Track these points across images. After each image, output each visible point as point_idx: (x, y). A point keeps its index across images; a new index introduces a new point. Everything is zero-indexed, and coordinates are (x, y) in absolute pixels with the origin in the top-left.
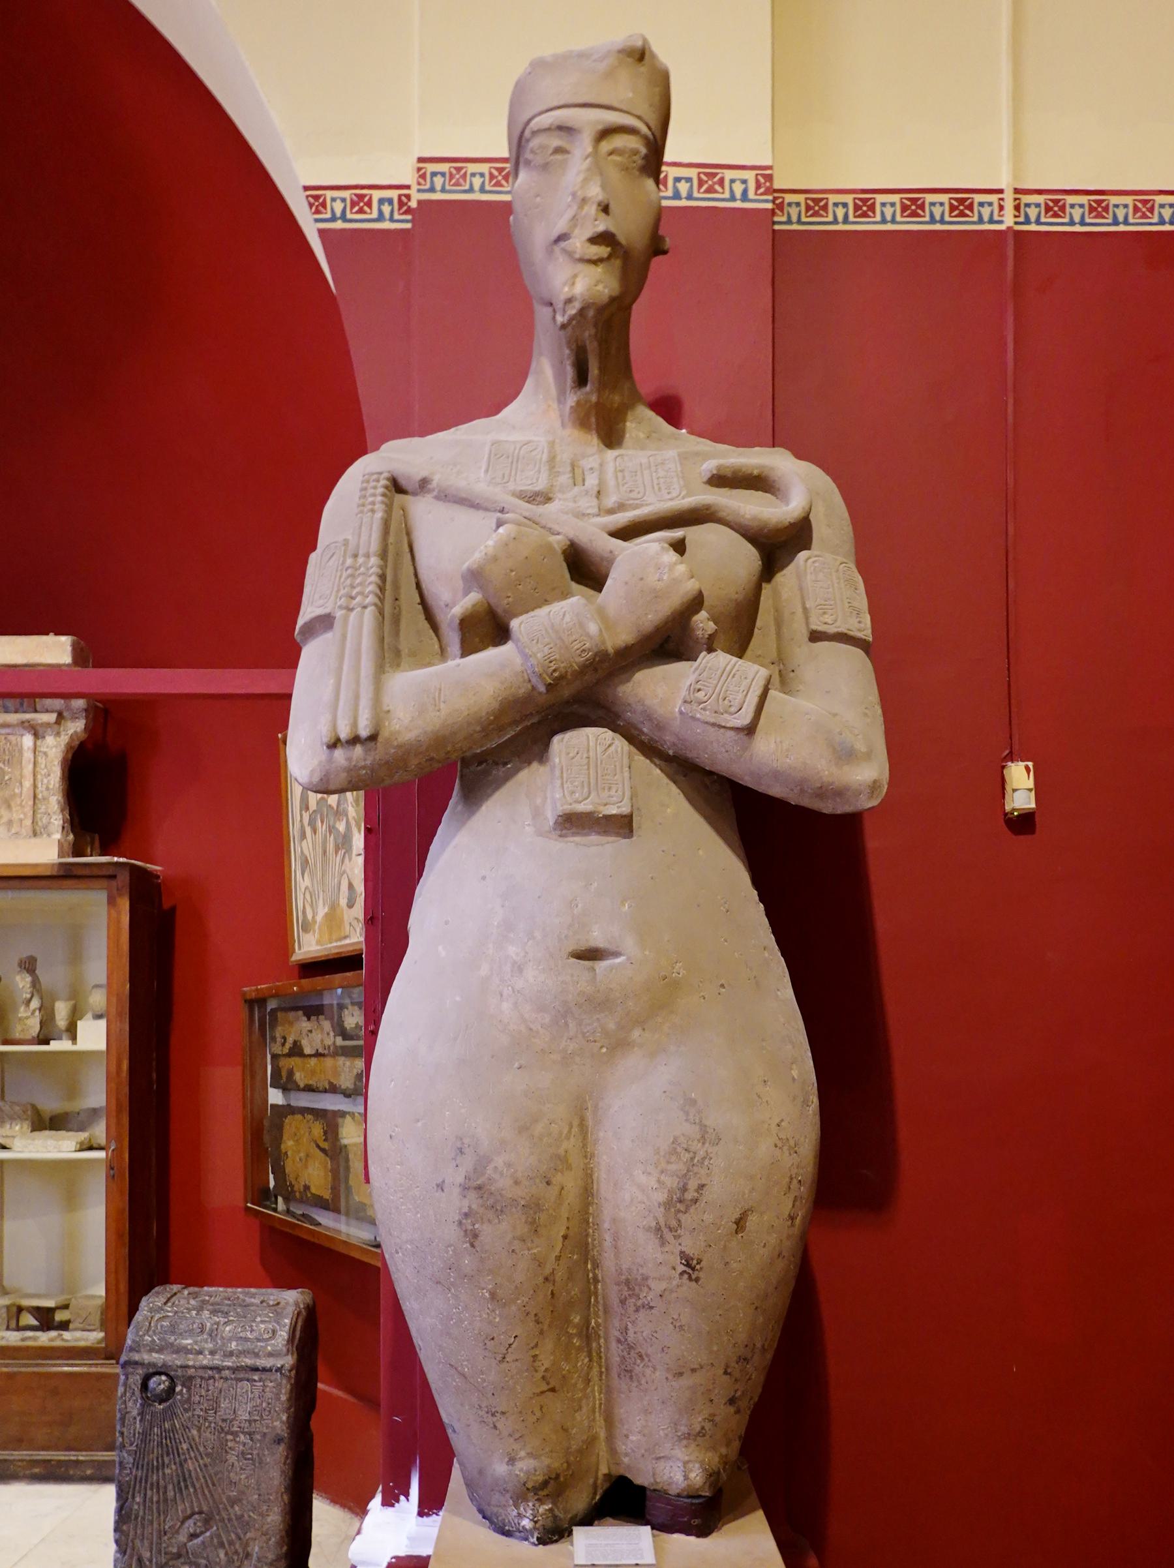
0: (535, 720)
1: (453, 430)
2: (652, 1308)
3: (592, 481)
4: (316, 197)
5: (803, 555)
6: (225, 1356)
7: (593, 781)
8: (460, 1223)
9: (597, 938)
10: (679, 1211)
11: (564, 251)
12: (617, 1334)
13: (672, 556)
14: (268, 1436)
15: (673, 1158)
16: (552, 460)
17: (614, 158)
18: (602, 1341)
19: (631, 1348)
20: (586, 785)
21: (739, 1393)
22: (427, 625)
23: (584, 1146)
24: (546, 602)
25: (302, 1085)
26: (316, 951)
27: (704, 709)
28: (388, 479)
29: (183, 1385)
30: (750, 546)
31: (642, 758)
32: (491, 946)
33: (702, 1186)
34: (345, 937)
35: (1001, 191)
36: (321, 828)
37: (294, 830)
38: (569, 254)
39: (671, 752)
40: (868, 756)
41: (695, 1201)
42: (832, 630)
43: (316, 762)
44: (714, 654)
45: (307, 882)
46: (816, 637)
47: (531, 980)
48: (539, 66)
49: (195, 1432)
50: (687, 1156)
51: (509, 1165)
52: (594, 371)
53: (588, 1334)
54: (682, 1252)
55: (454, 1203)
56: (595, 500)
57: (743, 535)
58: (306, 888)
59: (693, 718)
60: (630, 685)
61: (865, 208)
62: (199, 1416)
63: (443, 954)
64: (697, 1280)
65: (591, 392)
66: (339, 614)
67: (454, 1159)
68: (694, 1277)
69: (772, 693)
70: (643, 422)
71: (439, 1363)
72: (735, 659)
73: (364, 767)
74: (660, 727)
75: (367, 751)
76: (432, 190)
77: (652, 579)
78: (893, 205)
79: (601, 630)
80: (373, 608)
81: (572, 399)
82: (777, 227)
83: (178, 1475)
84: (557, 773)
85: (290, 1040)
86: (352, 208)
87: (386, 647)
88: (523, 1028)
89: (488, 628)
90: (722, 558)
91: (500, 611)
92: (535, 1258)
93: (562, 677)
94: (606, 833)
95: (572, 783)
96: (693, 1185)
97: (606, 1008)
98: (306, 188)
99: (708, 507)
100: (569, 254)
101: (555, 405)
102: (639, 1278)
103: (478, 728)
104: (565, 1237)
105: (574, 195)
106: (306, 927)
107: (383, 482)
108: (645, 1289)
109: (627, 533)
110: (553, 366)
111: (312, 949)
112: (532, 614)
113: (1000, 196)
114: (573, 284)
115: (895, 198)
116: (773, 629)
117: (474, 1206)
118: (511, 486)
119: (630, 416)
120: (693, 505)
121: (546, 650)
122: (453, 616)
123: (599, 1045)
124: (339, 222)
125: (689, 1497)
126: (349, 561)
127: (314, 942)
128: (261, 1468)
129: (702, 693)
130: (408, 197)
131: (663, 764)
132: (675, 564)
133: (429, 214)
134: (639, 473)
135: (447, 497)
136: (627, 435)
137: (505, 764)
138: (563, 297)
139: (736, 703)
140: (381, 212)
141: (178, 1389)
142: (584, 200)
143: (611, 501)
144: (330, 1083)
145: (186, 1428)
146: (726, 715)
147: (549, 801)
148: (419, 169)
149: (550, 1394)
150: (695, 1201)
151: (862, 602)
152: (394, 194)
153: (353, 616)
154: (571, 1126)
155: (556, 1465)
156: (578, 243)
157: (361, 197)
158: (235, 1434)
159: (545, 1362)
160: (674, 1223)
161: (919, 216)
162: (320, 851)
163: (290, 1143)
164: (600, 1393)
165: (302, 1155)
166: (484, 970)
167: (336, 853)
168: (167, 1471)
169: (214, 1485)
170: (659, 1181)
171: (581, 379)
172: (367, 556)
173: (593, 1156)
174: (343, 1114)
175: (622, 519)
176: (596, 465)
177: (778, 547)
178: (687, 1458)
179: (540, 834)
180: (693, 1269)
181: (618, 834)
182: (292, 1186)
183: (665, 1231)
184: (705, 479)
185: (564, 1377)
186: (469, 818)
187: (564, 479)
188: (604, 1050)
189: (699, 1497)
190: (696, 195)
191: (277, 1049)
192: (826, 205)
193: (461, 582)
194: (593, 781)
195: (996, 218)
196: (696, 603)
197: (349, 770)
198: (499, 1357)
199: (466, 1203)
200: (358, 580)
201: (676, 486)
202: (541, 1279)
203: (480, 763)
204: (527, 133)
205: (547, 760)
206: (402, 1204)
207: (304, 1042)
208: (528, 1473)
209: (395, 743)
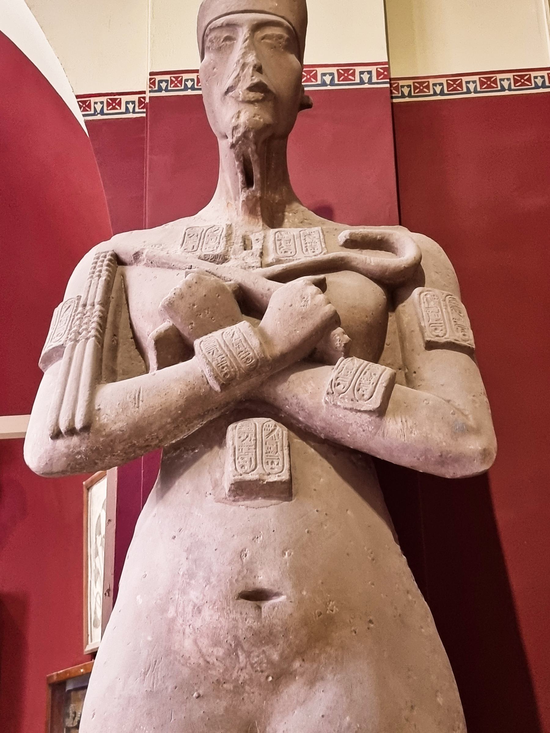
3: (257, 247)
4: (84, 101)
5: (417, 291)
7: (259, 457)
16: (229, 236)
20: (253, 460)
24: (221, 327)
28: (112, 255)
30: (376, 285)
31: (300, 441)
39: (322, 436)
40: (477, 431)
42: (443, 340)
46: (430, 346)
47: (208, 619)
52: (257, 175)
56: (259, 258)
57: (371, 278)
60: (286, 384)
61: (455, 86)
65: (256, 189)
70: (296, 213)
73: (79, 453)
76: (160, 90)
78: (474, 82)
79: (261, 344)
80: (94, 338)
81: (243, 196)
82: (395, 101)
86: (108, 106)
87: (103, 367)
88: (201, 661)
90: (354, 292)
93: (232, 379)
95: (242, 459)
98: (77, 97)
99: (342, 259)
103: (169, 420)
107: (108, 257)
112: (210, 335)
115: (476, 78)
116: (398, 344)
118: (198, 253)
123: (266, 674)
124: (99, 115)
129: (341, 386)
130: (144, 98)
131: (317, 445)
133: (156, 107)
134: (292, 241)
135: (152, 263)
137: (193, 450)
140: (127, 108)
143: (270, 259)
148: (150, 79)
151: (466, 322)
152: (135, 98)
156: (241, 90)
157: (114, 100)
166: (171, 613)
171: (248, 182)
175: (277, 268)
176: (261, 238)
177: (398, 285)
181: (279, 498)
184: (342, 243)
188: (270, 679)
192: (428, 85)
193: (158, 317)
194: (259, 457)
196: (334, 320)
209: (104, 433)
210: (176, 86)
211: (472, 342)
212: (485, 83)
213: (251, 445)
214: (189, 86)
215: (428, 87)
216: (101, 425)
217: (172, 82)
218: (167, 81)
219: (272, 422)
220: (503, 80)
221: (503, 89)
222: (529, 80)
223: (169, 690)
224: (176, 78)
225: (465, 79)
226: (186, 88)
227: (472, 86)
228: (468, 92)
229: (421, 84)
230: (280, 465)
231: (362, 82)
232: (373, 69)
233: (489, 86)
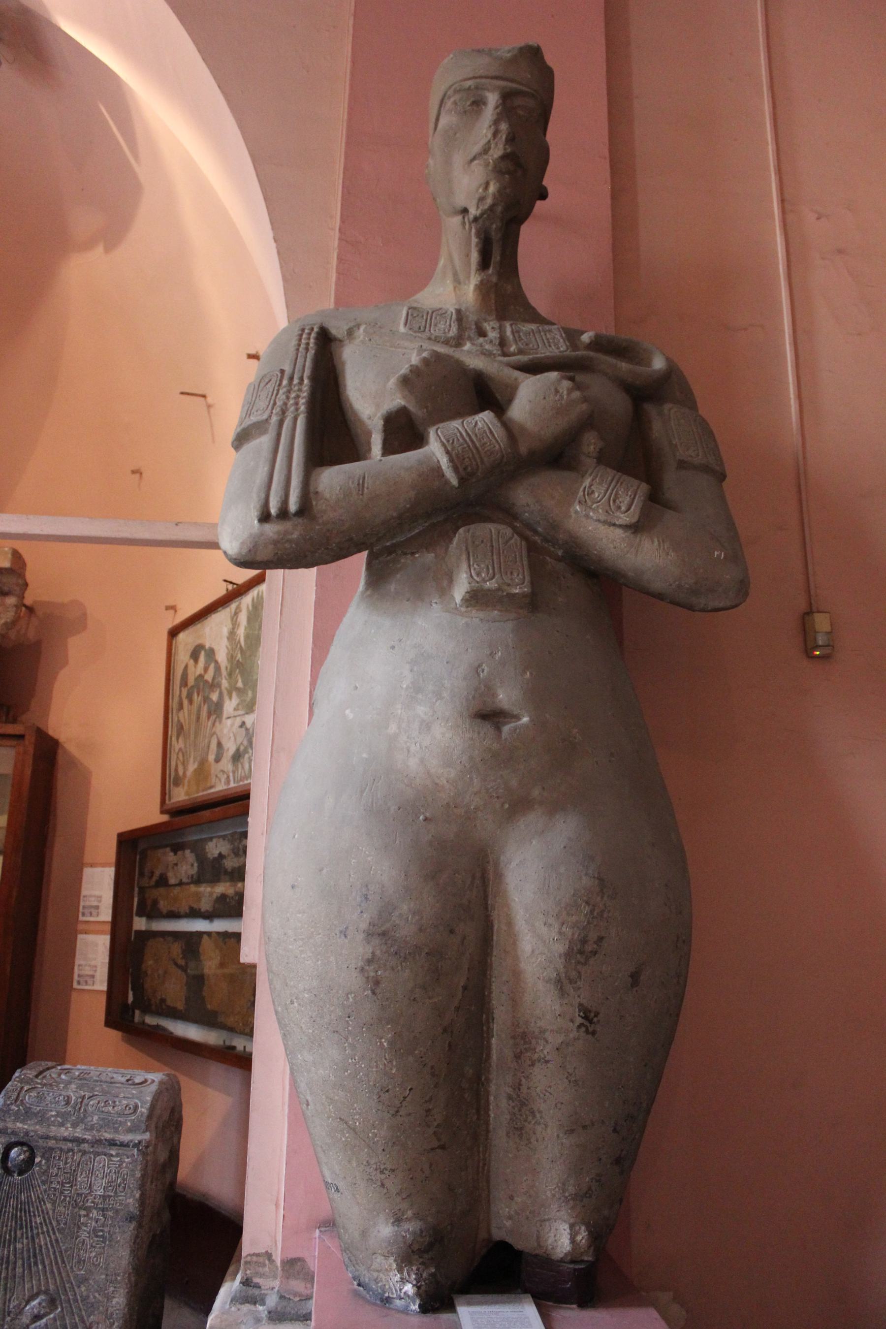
2: (547, 1062)
6: (86, 1129)
8: (362, 970)
10: (579, 962)
12: (509, 1090)
14: (121, 1213)
21: (624, 1152)
25: (165, 911)
26: (184, 801)
29: (43, 1157)
32: (399, 706)
33: (601, 939)
34: (211, 787)
41: (595, 953)
45: (181, 744)
49: (49, 1206)
54: (580, 1005)
58: (180, 750)
62: (55, 1189)
63: (351, 716)
64: (594, 1033)
68: (591, 1030)
71: (328, 1118)
83: (29, 1251)
85: (157, 873)
96: (593, 936)
102: (537, 1031)
104: (465, 988)
108: (542, 1042)
111: (180, 799)
117: (378, 952)
125: (572, 1262)
127: (183, 794)
128: (110, 1246)
141: (37, 1160)
144: (191, 908)
145: (41, 1201)
149: (439, 1151)
150: (595, 953)
154: (474, 877)
158: (88, 1210)
162: (194, 717)
163: (151, 962)
165: (161, 972)
166: (393, 728)
167: (209, 718)
168: (19, 1246)
169: (63, 1262)
178: (572, 1221)
180: (591, 1022)
189: (582, 1261)
191: (145, 882)
198: (392, 1112)
207: (170, 874)
208: (414, 1233)
223: (392, 811)
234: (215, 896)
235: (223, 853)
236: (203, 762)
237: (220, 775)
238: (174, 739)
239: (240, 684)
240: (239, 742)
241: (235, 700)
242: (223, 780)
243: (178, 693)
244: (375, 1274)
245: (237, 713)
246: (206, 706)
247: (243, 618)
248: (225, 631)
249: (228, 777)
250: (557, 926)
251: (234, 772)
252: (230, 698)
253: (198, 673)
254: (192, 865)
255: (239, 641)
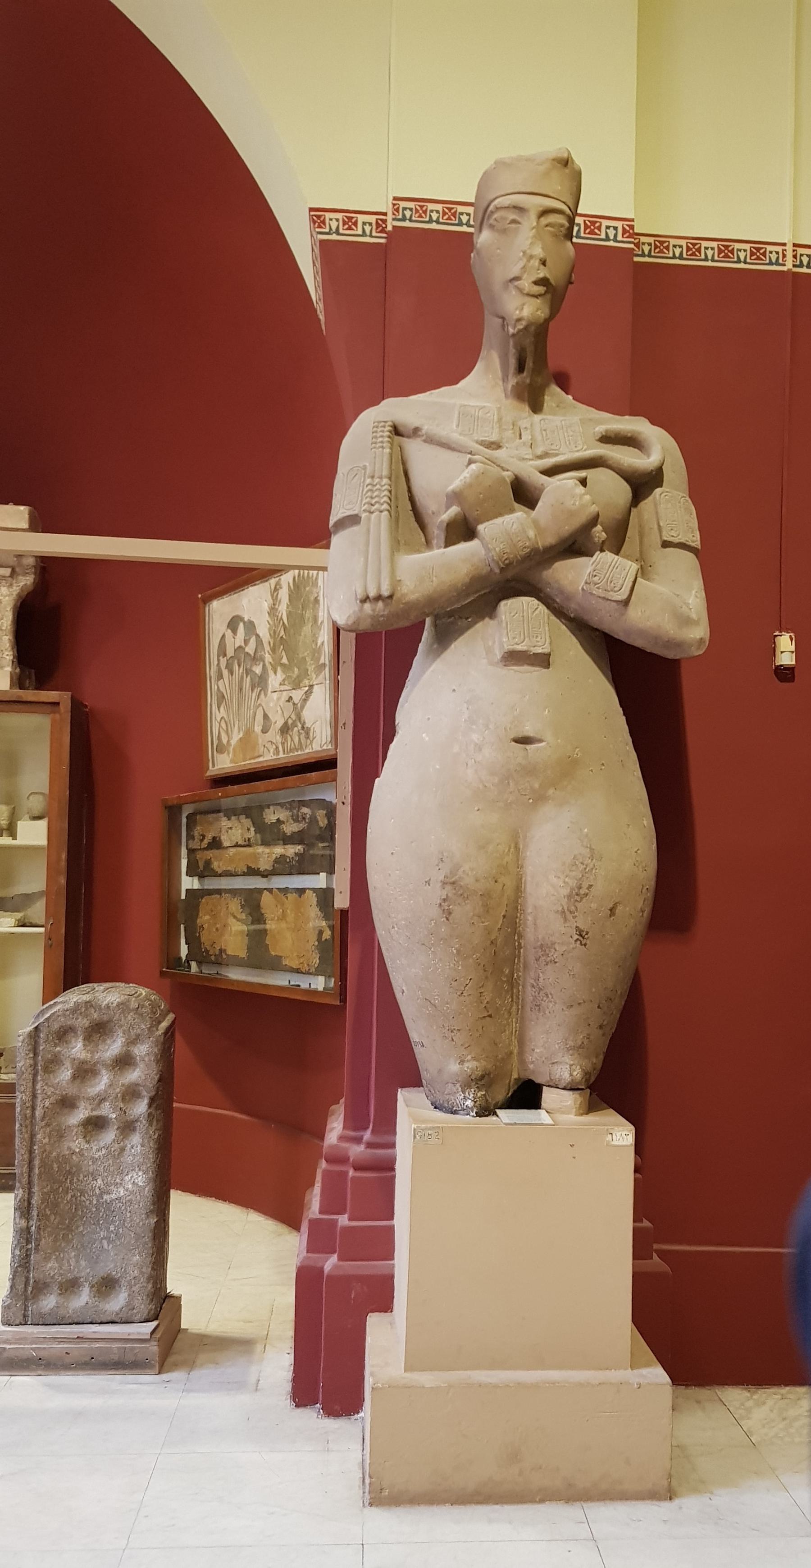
0: (486, 591)
1: (428, 393)
2: (556, 962)
5: (658, 491)
9: (528, 730)
11: (517, 288)
12: (532, 981)
13: (581, 489)
15: (574, 868)
16: (500, 420)
17: (549, 228)
18: (520, 987)
19: (541, 989)
22: (416, 525)
23: (518, 860)
24: (500, 515)
27: (598, 588)
34: (259, 756)
35: (784, 244)
36: (238, 671)
37: (211, 672)
38: (520, 290)
39: (572, 615)
40: (697, 623)
41: (587, 894)
42: (676, 540)
43: (351, 612)
44: (604, 553)
46: (666, 544)
48: (500, 164)
50: (583, 867)
51: (472, 869)
52: (529, 364)
53: (512, 983)
55: (437, 893)
57: (621, 476)
59: (591, 594)
60: (550, 571)
64: (585, 945)
66: (364, 515)
67: (438, 865)
69: (638, 579)
72: (613, 555)
73: (382, 616)
74: (568, 598)
75: (386, 605)
76: (404, 219)
77: (569, 503)
81: (512, 381)
84: (504, 624)
88: (481, 786)
89: (462, 530)
90: (611, 490)
91: (471, 519)
92: (486, 928)
94: (532, 665)
96: (585, 885)
97: (532, 776)
99: (601, 457)
100: (520, 290)
101: (501, 383)
104: (504, 916)
105: (524, 253)
106: (221, 749)
109: (550, 472)
110: (500, 357)
111: (225, 766)
113: (784, 248)
114: (522, 309)
119: (547, 392)
120: (592, 455)
121: (501, 546)
122: (442, 522)
123: (528, 797)
126: (368, 481)
130: (384, 221)
131: (567, 622)
132: (584, 494)
136: (545, 405)
137: (467, 618)
138: (515, 317)
139: (619, 586)
142: (531, 257)
144: (249, 868)
146: (611, 593)
147: (497, 643)
152: (372, 219)
153: (373, 516)
154: (510, 848)
155: (489, 1066)
157: (350, 218)
159: (487, 997)
160: (573, 908)
161: (729, 257)
164: (516, 1023)
166: (456, 749)
167: (252, 690)
170: (564, 882)
171: (521, 368)
172: (381, 478)
173: (522, 867)
174: (260, 891)
176: (528, 426)
177: (643, 484)
179: (491, 664)
180: (583, 938)
182: (207, 951)
183: (567, 913)
184: (597, 438)
185: (497, 1008)
186: (442, 653)
187: (509, 433)
188: (531, 801)
190: (582, 235)
191: (195, 845)
192: (668, 246)
195: (781, 261)
196: (594, 521)
197: (373, 617)
199: (444, 893)
200: (376, 494)
201: (580, 442)
202: (489, 942)
203: (450, 617)
204: (491, 207)
205: (495, 617)
206: (400, 895)
210: (420, 216)
211: (699, 543)
212: (723, 251)
213: (521, 619)
214: (434, 218)
215: (667, 248)
216: (402, 595)
217: (417, 211)
218: (411, 210)
219: (536, 602)
220: (740, 250)
221: (739, 261)
222: (764, 254)
224: (421, 207)
225: (705, 244)
226: (431, 221)
227: (710, 253)
228: (706, 259)
229: (662, 243)
230: (543, 640)
231: (607, 239)
232: (619, 224)
233: (726, 256)
234: (274, 856)
235: (281, 819)
236: (249, 732)
237: (269, 745)
238: (215, 707)
239: (285, 660)
240: (286, 716)
241: (280, 676)
242: (272, 751)
243: (216, 662)
244: (447, 1097)
245: (282, 688)
246: (249, 678)
247: (284, 595)
248: (266, 606)
249: (277, 748)
250: (562, 877)
251: (283, 744)
252: (275, 673)
253: (237, 645)
254: (249, 829)
255: (281, 618)
